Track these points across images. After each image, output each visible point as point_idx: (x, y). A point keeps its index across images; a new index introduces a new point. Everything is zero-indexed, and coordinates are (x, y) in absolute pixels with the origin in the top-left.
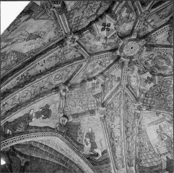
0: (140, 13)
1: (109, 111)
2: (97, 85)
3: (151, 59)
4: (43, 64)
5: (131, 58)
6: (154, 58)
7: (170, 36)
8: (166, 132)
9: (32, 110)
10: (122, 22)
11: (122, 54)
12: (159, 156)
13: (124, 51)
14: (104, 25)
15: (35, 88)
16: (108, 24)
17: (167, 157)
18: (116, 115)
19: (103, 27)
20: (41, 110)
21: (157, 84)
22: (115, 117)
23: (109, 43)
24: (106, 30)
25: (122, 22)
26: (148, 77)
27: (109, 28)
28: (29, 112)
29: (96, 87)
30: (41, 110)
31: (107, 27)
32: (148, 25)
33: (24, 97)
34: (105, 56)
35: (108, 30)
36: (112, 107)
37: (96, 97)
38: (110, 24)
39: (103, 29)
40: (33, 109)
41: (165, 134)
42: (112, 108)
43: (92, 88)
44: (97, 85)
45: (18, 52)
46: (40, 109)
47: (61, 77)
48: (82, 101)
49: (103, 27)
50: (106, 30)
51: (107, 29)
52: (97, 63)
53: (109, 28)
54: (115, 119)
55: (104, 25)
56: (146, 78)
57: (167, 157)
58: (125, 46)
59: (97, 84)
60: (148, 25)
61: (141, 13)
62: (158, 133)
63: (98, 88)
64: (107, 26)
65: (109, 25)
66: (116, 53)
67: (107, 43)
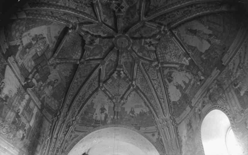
0: (141, 60)
2: (118, 9)
3: (104, 46)
5: (116, 39)
6: (103, 47)
8: (39, 42)
12: (20, 37)
14: (153, 45)
17: (19, 45)
18: (78, 5)
21: (86, 45)
22: (77, 4)
24: (149, 43)
26: (95, 42)
31: (150, 44)
35: (147, 44)
36: (88, 5)
39: (150, 42)
41: (37, 41)
44: (118, 9)
50: (149, 43)
51: (149, 44)
54: (75, 3)
56: (95, 41)
57: (19, 45)
58: (127, 41)
61: (140, 61)
62: (39, 35)
63: (115, 8)
65: (149, 46)
67: (137, 33)
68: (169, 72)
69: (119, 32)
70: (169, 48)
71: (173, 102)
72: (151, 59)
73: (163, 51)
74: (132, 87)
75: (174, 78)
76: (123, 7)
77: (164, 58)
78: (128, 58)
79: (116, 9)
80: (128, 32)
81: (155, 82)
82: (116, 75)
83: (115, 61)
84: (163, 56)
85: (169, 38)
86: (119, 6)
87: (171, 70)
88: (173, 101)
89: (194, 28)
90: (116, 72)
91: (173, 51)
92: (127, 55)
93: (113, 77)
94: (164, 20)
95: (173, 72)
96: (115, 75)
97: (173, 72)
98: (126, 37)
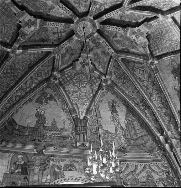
1: (163, 6)
2: (137, 32)
4: (131, 92)
7: (50, 9)
9: (176, 87)
10: (73, 52)
11: (95, 30)
13: (91, 31)
14: (83, 66)
15: (154, 91)
16: (81, 64)
19: (85, 65)
20: (176, 78)
23: (94, 44)
25: (73, 52)
27: (83, 62)
28: (176, 91)
29: (140, 32)
30: (176, 78)
32: (59, 31)
33: (162, 99)
34: (105, 44)
37: (150, 28)
38: (80, 63)
40: (175, 87)
42: (157, 4)
43: (141, 35)
45: (126, 114)
46: (175, 79)
47: (141, 69)
48: (163, 34)
49: (85, 65)
52: (116, 41)
53: (83, 62)
55: (83, 66)
59: (136, 33)
60: (59, 31)
63: (139, 29)
64: (82, 64)
66: (98, 36)
67: (95, 45)
68: (51, 95)
69: (102, 26)
70: (83, 86)
71: (13, 119)
72: (60, 67)
73: (74, 79)
74: (9, 50)
75: (48, 106)
76: (137, 38)
77: (68, 83)
78: (54, 33)
79: (137, 30)
80: (99, 36)
81: (28, 83)
82: (26, 20)
83: (50, 13)
84: (68, 81)
85: (95, 85)
86: (140, 33)
87: (56, 98)
88: (14, 119)
89: (117, 109)
90: (33, 19)
91: (82, 92)
92: (60, 32)
93: (23, 13)
94: (117, 76)
95: (55, 100)
96: (27, 17)
97: (55, 100)
98: (93, 34)
